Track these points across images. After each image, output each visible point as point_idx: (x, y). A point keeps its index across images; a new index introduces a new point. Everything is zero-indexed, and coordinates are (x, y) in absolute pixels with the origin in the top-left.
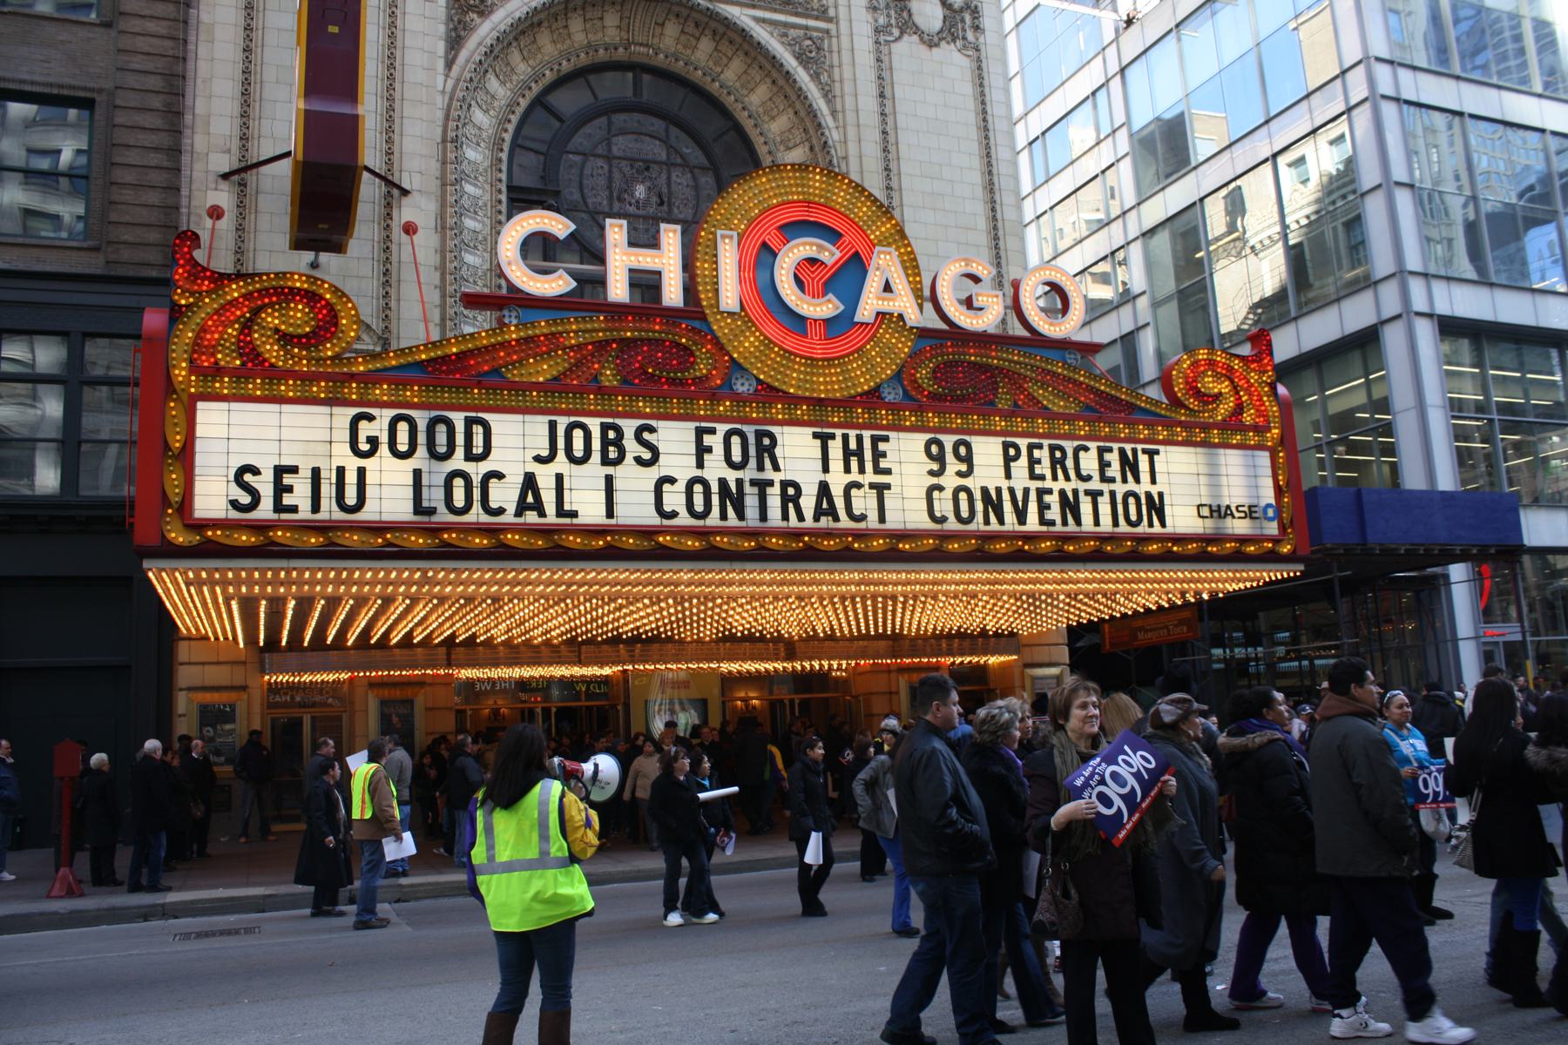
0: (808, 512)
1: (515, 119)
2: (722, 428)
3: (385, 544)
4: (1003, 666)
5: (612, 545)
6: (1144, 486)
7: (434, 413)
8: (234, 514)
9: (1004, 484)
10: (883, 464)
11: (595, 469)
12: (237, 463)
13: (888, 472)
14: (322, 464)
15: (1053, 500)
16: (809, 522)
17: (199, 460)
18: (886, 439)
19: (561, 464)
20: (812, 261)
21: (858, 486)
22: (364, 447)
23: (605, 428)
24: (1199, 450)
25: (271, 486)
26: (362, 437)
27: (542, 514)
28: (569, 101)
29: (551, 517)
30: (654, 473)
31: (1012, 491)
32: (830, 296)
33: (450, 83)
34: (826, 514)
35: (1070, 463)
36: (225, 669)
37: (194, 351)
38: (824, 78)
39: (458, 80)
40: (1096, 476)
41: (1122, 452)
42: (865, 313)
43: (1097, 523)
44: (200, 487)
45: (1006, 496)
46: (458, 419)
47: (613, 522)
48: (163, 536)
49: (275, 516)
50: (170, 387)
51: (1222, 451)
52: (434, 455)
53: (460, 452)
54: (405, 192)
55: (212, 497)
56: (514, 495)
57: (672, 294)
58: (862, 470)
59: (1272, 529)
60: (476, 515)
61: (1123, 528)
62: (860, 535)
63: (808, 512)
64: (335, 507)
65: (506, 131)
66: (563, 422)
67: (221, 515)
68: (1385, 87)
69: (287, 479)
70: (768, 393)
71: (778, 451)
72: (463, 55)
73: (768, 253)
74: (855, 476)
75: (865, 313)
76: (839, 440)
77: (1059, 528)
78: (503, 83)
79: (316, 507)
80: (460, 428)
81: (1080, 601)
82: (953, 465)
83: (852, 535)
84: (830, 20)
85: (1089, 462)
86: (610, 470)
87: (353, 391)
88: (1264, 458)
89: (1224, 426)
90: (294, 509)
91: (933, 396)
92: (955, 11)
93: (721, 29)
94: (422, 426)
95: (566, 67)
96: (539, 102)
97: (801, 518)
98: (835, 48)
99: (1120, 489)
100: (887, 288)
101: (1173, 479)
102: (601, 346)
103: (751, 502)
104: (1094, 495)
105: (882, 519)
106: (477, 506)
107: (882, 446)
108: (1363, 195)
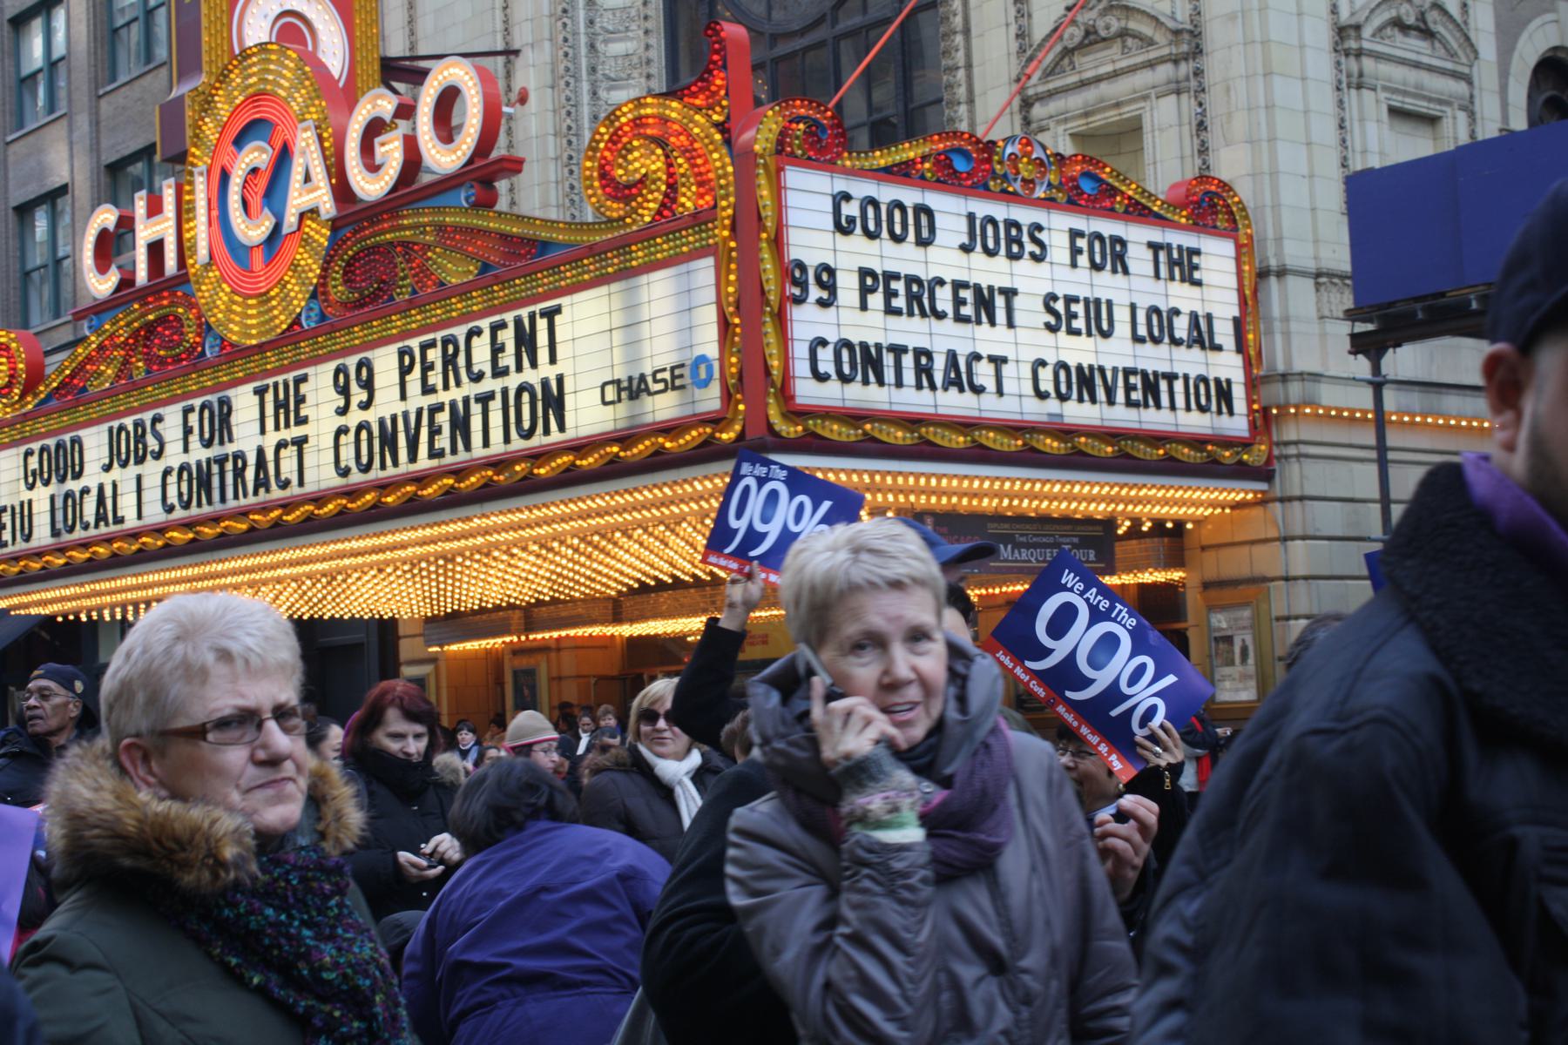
2: (197, 402)
6: (546, 371)
10: (303, 413)
11: (133, 470)
15: (443, 418)
16: (251, 500)
18: (304, 379)
19: (117, 471)
20: (255, 171)
24: (615, 287)
30: (160, 466)
31: (406, 415)
35: (461, 360)
40: (487, 369)
41: (518, 322)
42: (291, 220)
43: (486, 443)
51: (644, 279)
54: (516, 52)
59: (710, 399)
60: (79, 534)
61: (518, 444)
62: (287, 506)
70: (233, 353)
71: (234, 419)
73: (225, 176)
75: (291, 220)
76: (271, 390)
77: (449, 459)
81: (495, 559)
82: (358, 395)
83: (283, 506)
88: (704, 270)
91: (346, 305)
97: (245, 495)
99: (513, 381)
100: (307, 179)
101: (582, 347)
102: (135, 334)
104: (485, 399)
105: (301, 483)
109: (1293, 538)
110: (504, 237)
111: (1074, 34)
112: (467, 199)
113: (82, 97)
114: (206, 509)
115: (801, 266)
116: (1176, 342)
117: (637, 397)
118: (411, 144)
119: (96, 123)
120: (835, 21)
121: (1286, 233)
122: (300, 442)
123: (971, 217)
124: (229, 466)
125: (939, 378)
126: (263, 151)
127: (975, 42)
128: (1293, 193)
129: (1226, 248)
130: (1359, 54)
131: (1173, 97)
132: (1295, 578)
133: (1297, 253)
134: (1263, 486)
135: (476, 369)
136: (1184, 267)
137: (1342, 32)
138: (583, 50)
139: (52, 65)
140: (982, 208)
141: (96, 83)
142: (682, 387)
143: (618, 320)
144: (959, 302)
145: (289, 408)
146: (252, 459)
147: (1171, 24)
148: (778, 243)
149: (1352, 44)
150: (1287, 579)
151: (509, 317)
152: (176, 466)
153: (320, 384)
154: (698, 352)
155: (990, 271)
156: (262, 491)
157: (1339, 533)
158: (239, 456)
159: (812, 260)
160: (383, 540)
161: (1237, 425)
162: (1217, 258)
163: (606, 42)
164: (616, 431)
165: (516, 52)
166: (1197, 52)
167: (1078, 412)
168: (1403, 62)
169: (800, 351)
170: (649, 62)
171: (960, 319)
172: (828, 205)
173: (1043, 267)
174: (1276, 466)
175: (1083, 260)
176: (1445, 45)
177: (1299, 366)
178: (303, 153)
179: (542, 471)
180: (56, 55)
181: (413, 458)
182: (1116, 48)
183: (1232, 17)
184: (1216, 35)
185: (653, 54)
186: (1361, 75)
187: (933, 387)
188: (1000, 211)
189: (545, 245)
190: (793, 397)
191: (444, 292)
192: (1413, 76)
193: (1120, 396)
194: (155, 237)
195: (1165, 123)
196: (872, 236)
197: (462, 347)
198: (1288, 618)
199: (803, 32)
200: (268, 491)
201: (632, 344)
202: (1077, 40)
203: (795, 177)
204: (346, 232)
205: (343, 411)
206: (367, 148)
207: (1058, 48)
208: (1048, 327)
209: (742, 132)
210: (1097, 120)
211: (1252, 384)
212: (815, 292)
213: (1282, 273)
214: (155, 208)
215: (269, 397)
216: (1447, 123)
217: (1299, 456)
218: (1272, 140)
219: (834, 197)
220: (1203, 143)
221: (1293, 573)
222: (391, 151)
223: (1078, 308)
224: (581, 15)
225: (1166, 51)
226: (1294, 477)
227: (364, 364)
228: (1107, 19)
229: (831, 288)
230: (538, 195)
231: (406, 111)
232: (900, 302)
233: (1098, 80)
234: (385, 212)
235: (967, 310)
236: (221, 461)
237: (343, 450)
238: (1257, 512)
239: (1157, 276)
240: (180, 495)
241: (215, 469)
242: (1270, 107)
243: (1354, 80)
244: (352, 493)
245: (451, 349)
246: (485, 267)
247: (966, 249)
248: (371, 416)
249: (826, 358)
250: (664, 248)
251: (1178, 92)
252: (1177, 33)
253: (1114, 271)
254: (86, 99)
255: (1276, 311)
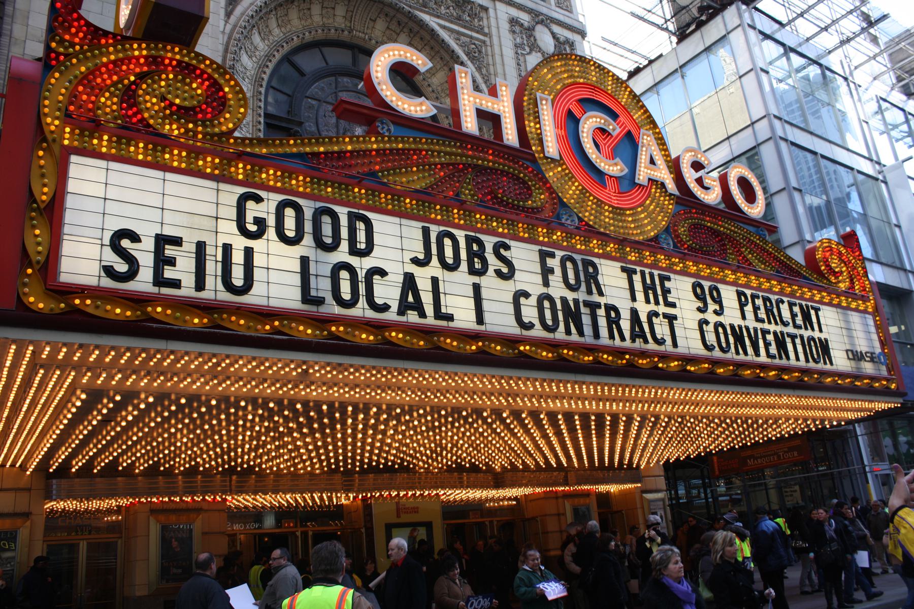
0: (627, 334)
1: (271, 66)
2: (559, 254)
3: (270, 332)
4: (623, 493)
5: (484, 351)
7: (319, 204)
8: (107, 283)
9: (742, 323)
12: (116, 225)
13: (673, 305)
14: (208, 239)
16: (628, 344)
17: (69, 217)
19: (434, 269)
21: (656, 314)
22: (253, 228)
23: (470, 240)
25: (151, 256)
26: (249, 218)
27: (423, 315)
28: (310, 62)
29: (430, 320)
30: (510, 287)
31: (747, 329)
32: (618, 160)
33: (229, 27)
34: (639, 336)
36: (10, 496)
37: (71, 103)
38: (484, 71)
39: (235, 26)
44: (67, 247)
46: (343, 212)
47: (482, 328)
48: (19, 299)
49: (155, 290)
50: (40, 135)
52: (320, 244)
53: (344, 246)
55: (82, 260)
56: (396, 293)
57: (510, 136)
58: (657, 303)
60: (361, 310)
62: (664, 357)
63: (627, 334)
64: (220, 287)
65: (265, 73)
66: (434, 230)
67: (93, 282)
68: (780, 133)
69: (170, 251)
71: (600, 277)
72: (239, 10)
74: (652, 307)
78: (263, 39)
79: (200, 285)
80: (344, 221)
82: (712, 306)
84: (485, 35)
86: (476, 279)
87: (240, 170)
90: (176, 284)
91: (690, 248)
92: (560, 43)
93: (416, 28)
94: (308, 214)
95: (308, 37)
96: (287, 59)
98: (490, 53)
103: (586, 320)
106: (362, 302)
107: (667, 284)
108: (772, 195)
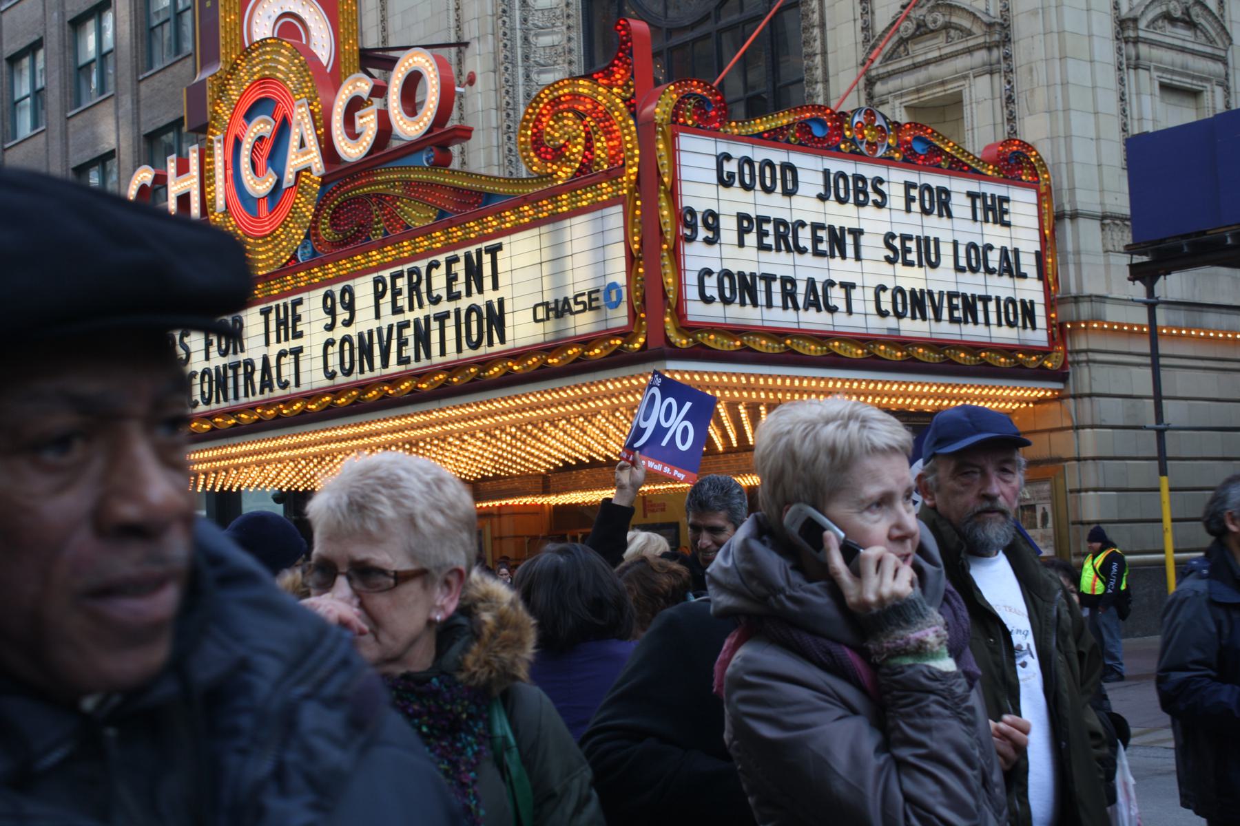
6: (490, 295)
10: (299, 329)
15: (409, 333)
16: (258, 397)
18: (300, 302)
20: (261, 138)
24: (544, 229)
31: (380, 330)
35: (423, 287)
40: (444, 294)
41: (468, 257)
42: (289, 177)
43: (443, 353)
45: (376, 339)
51: (567, 222)
54: (466, 44)
59: (620, 317)
61: (468, 353)
62: (288, 401)
73: (238, 143)
74: (286, 346)
75: (289, 177)
76: (274, 311)
77: (413, 365)
81: (450, 444)
82: (343, 315)
83: (284, 402)
85: (439, 280)
88: (615, 216)
89: (571, 186)
91: (334, 244)
97: (254, 394)
99: (464, 304)
100: (302, 144)
101: (518, 276)
104: (442, 318)
105: (297, 384)
109: (1083, 427)
110: (457, 190)
111: (908, 27)
112: (427, 160)
113: (126, 80)
114: (223, 404)
115: (692, 212)
116: (990, 271)
117: (562, 316)
118: (383, 117)
119: (137, 101)
120: (718, 18)
121: (1077, 185)
122: (297, 352)
123: (826, 173)
124: (241, 371)
125: (801, 300)
126: (268, 123)
127: (829, 35)
128: (1083, 152)
129: (1030, 196)
130: (1136, 41)
131: (987, 77)
132: (1085, 459)
133: (1086, 200)
134: (1060, 386)
135: (435, 295)
136: (997, 211)
137: (1124, 25)
138: (519, 42)
139: (102, 56)
140: (835, 166)
141: (137, 70)
142: (598, 308)
143: (547, 255)
144: (816, 240)
145: (289, 325)
146: (259, 365)
147: (986, 19)
148: (673, 194)
149: (1131, 34)
150: (1079, 459)
151: (461, 253)
152: (199, 370)
153: (312, 307)
154: (610, 280)
155: (841, 215)
156: (267, 390)
157: (1121, 423)
158: (248, 363)
159: (700, 207)
160: (362, 429)
161: (1039, 336)
162: (1023, 205)
163: (537, 35)
164: (545, 342)
165: (466, 44)
166: (1007, 40)
167: (912, 327)
168: (1171, 47)
169: (691, 279)
170: (570, 51)
171: (817, 253)
172: (713, 163)
173: (885, 211)
174: (1070, 370)
175: (916, 206)
176: (1205, 33)
177: (1089, 289)
178: (299, 125)
179: (424, 386)
180: (106, 48)
181: (385, 364)
182: (942, 38)
183: (1034, 12)
184: (1023, 27)
185: (574, 45)
186: (1138, 58)
187: (796, 308)
188: (849, 168)
189: (489, 196)
190: (685, 316)
191: (411, 233)
192: (1179, 58)
193: (945, 314)
194: (183, 191)
195: (981, 97)
196: (747, 188)
197: (424, 277)
198: (1079, 491)
199: (693, 27)
200: (271, 390)
201: (558, 274)
202: (910, 32)
203: (687, 142)
204: (331, 186)
205: (330, 328)
206: (349, 121)
207: (895, 38)
208: (888, 259)
209: (645, 105)
210: (927, 95)
211: (1050, 304)
212: (702, 233)
213: (1074, 216)
214: (183, 169)
215: (273, 316)
216: (1207, 96)
217: (1088, 362)
218: (1067, 110)
219: (717, 157)
220: (1011, 113)
221: (1083, 455)
222: (368, 123)
223: (912, 245)
224: (517, 14)
225: (981, 40)
226: (1084, 378)
227: (348, 290)
228: (934, 15)
229: (715, 229)
230: (482, 156)
231: (380, 91)
232: (770, 240)
233: (927, 63)
234: (364, 170)
235: (823, 247)
236: (235, 367)
237: (330, 358)
238: (1055, 407)
239: (975, 219)
240: (203, 393)
241: (230, 373)
242: (1065, 84)
243: (1132, 62)
244: (336, 392)
245: (415, 278)
246: (442, 214)
247: (822, 198)
248: (352, 331)
249: (711, 283)
250: (586, 199)
251: (991, 73)
252: (990, 25)
253: (940, 215)
254: (129, 83)
255: (1070, 247)
